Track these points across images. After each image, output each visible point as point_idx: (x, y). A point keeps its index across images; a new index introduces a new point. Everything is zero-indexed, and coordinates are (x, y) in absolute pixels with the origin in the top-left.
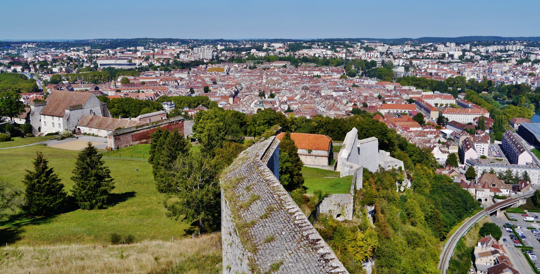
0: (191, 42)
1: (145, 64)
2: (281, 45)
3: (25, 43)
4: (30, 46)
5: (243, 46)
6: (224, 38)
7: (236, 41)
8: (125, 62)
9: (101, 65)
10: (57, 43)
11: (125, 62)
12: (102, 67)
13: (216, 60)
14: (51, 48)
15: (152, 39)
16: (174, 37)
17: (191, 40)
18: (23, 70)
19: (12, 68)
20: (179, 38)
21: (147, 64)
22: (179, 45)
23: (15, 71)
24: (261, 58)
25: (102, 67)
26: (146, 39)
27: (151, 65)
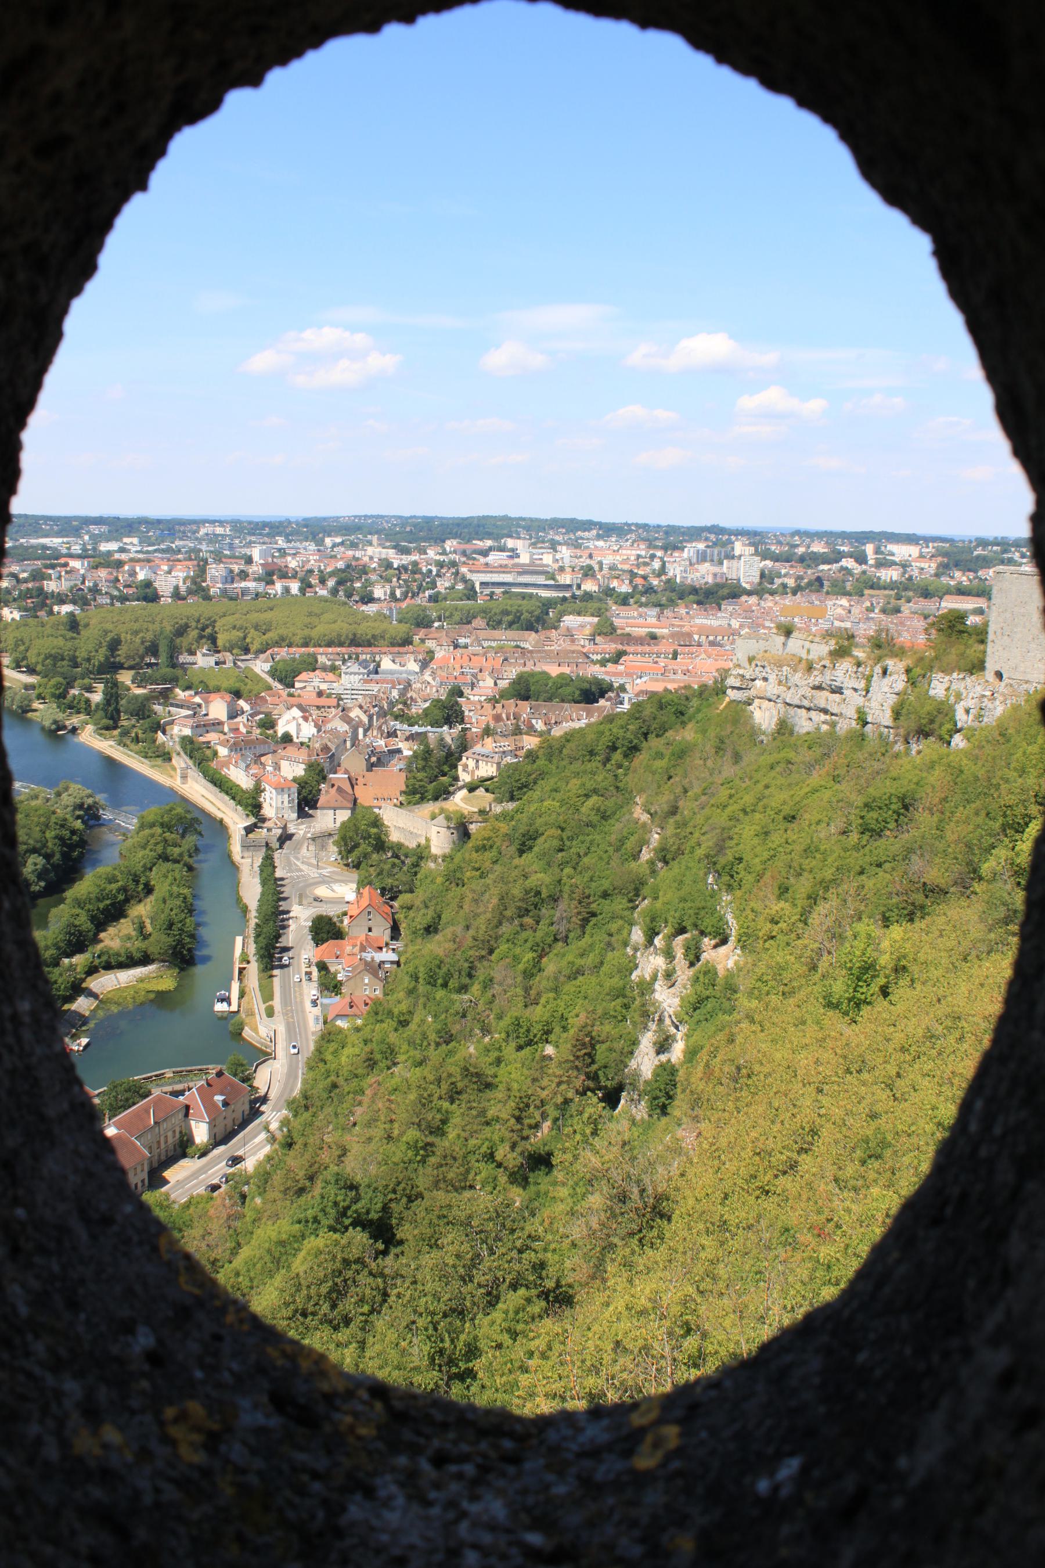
0: (630, 531)
1: (589, 586)
2: (913, 551)
3: (200, 522)
4: (219, 530)
5: (801, 550)
6: (723, 524)
7: (756, 534)
8: (541, 580)
9: (482, 584)
10: (281, 523)
11: (541, 580)
12: (487, 591)
13: (765, 585)
14: (272, 535)
15: (524, 519)
16: (582, 516)
17: (629, 525)
18: (303, 591)
19: (279, 586)
20: (596, 520)
21: (596, 588)
22: (599, 537)
23: (287, 590)
24: (892, 585)
25: (487, 591)
26: (506, 518)
27: (609, 592)
